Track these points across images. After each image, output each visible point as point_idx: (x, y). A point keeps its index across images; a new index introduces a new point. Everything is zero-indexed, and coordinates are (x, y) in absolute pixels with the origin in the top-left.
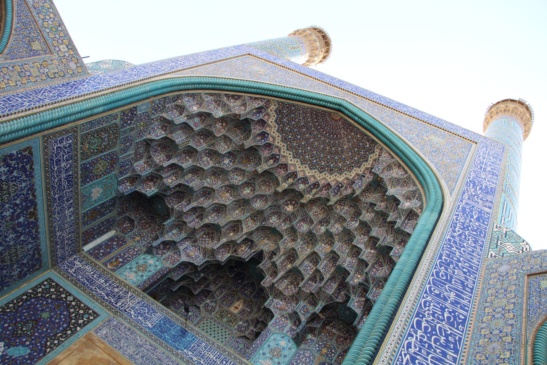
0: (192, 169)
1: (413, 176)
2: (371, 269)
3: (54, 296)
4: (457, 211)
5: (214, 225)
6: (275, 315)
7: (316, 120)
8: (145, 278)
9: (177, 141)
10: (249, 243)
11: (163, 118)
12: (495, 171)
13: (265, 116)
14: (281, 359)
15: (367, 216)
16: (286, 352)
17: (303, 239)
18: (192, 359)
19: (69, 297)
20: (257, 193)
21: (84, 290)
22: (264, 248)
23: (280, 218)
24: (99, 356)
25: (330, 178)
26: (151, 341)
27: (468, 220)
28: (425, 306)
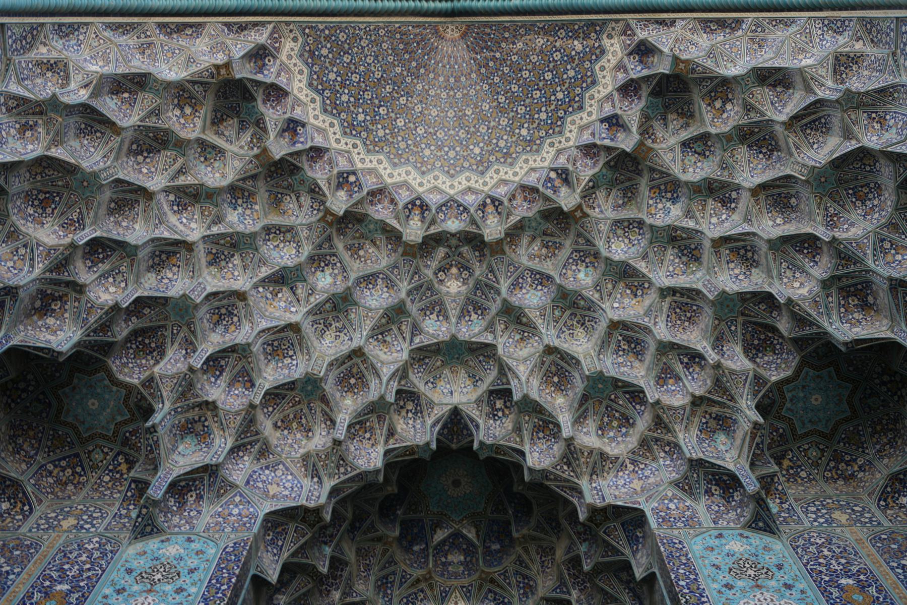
0: (153, 255)
5: (291, 385)
6: (641, 507)
7: (407, 56)
9: (85, 164)
10: (410, 406)
11: (15, 97)
13: (279, 75)
15: (694, 171)
16: (770, 560)
20: (353, 276)
23: (447, 318)
25: (515, 174)
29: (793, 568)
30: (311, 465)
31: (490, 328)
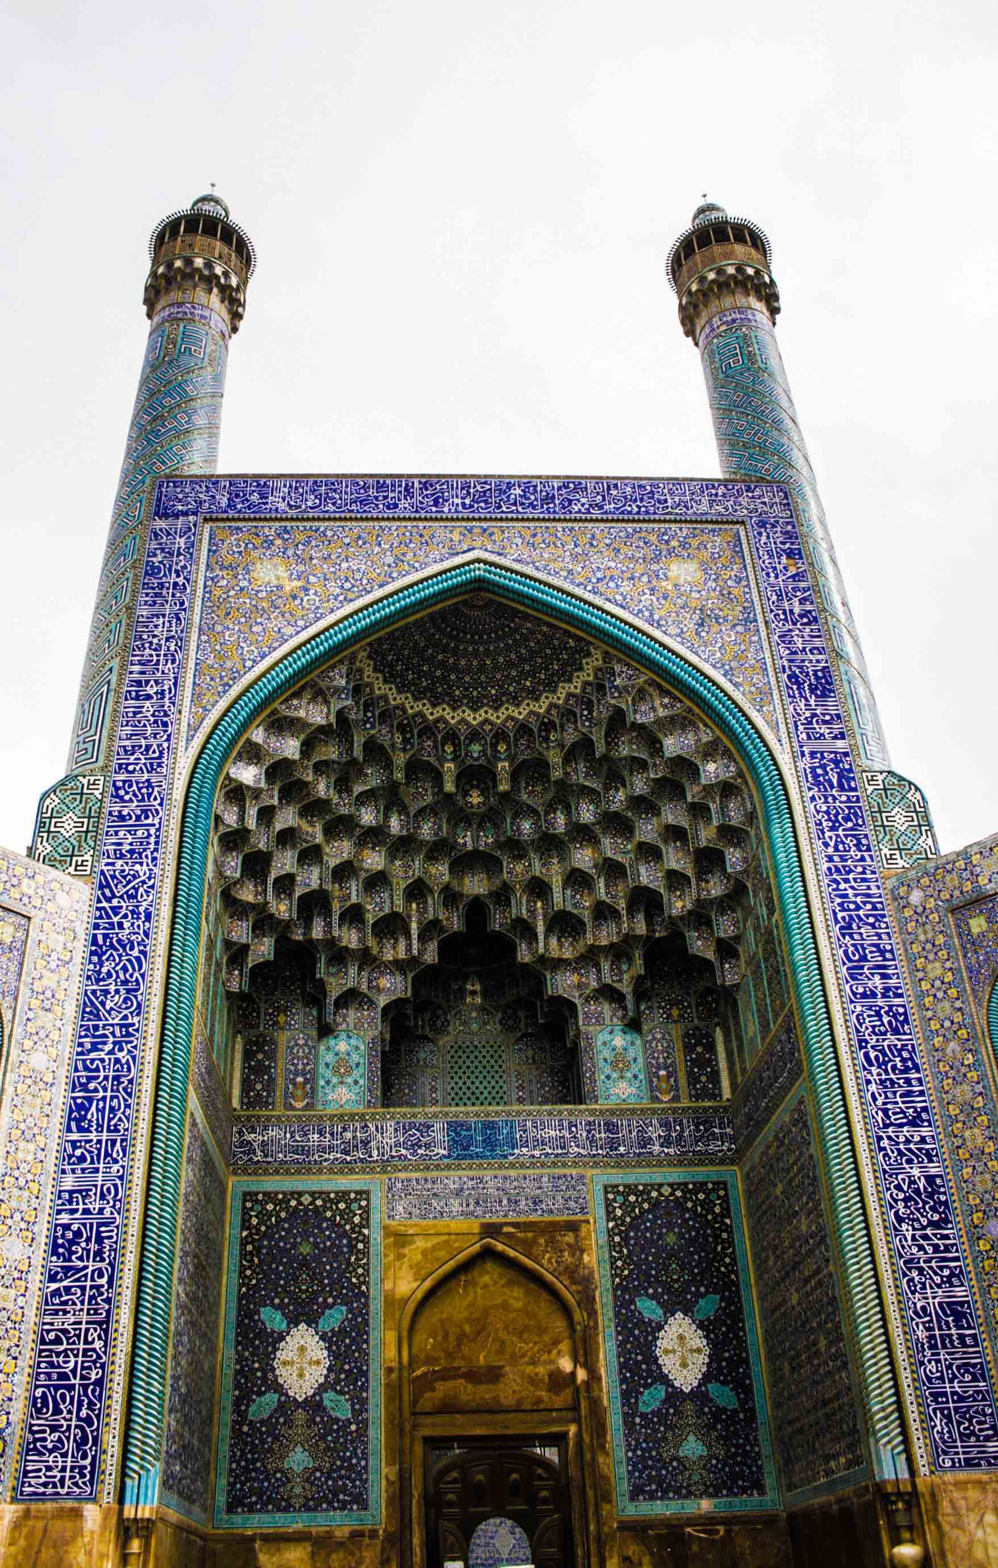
1: (697, 710)
2: (698, 885)
3: (283, 1215)
4: (810, 789)
8: (362, 1082)
12: (808, 607)
14: (635, 1068)
16: (631, 1054)
17: (538, 849)
18: (533, 1156)
19: (302, 1199)
20: (412, 811)
21: (309, 1171)
22: (476, 892)
23: (470, 825)
24: (429, 1244)
25: (520, 713)
26: (465, 1173)
27: (830, 799)
28: (861, 1025)
29: (640, 1060)
30: (399, 966)
31: (498, 845)
